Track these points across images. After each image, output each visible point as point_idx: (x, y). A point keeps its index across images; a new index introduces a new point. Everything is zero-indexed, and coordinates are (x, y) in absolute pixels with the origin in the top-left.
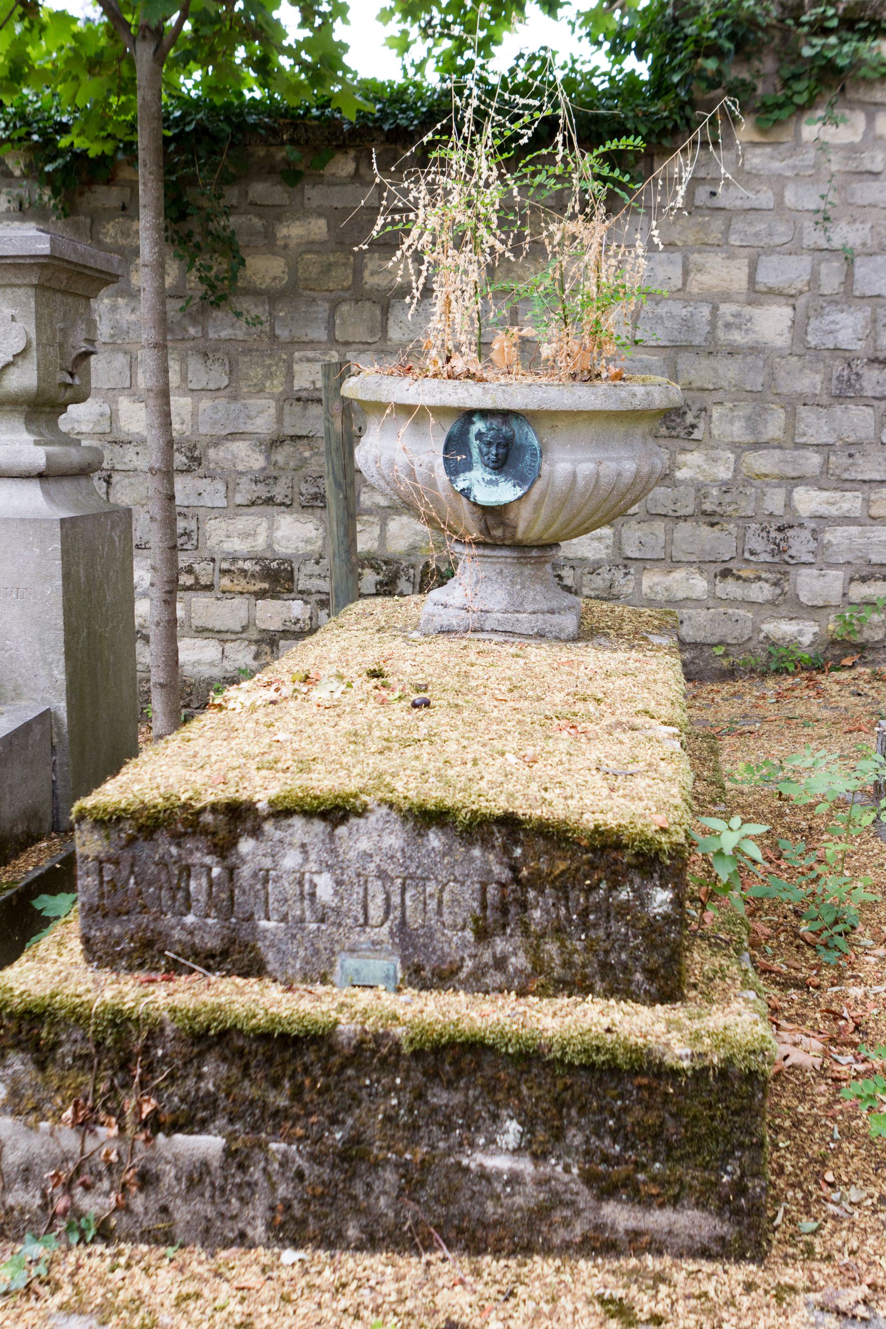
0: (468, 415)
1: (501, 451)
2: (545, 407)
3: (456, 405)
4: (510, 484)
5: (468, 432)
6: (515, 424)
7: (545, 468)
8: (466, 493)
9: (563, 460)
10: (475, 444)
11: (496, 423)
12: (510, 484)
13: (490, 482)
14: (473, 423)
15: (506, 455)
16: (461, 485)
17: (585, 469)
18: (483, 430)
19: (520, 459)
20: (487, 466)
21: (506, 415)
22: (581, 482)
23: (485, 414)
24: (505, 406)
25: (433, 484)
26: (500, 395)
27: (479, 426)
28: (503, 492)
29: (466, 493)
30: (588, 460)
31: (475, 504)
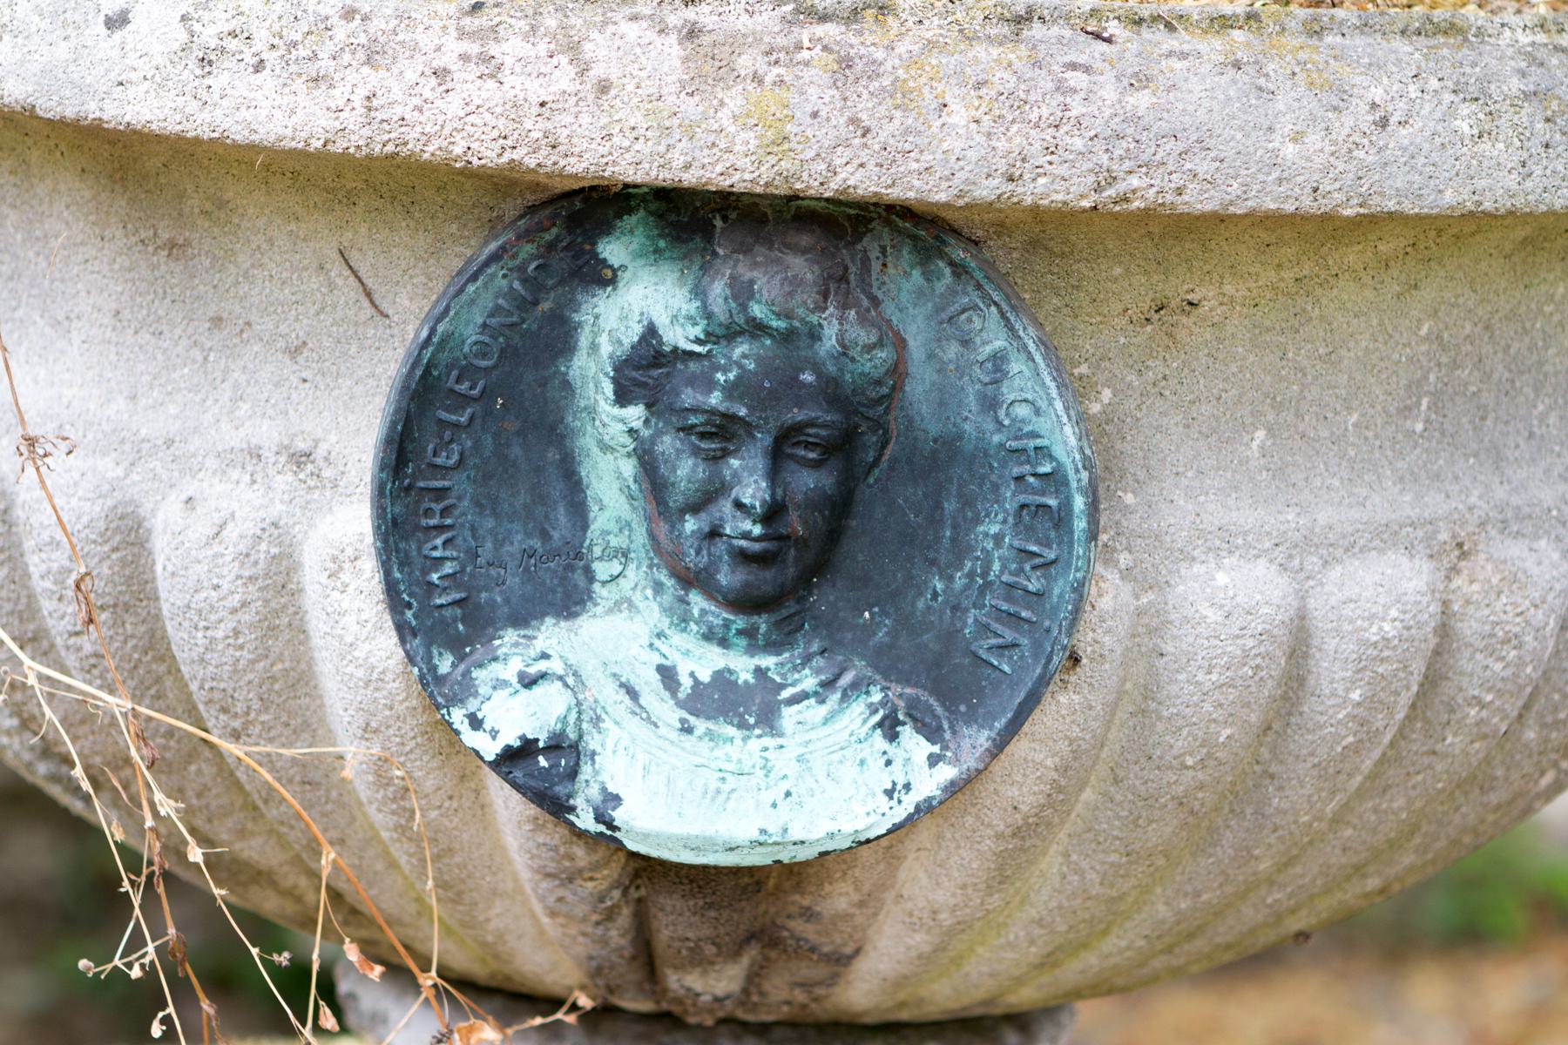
0: (571, 223)
1: (807, 481)
2: (1143, 189)
3: (489, 155)
4: (857, 716)
5: (558, 338)
6: (907, 291)
7: (1111, 595)
8: (542, 771)
9: (1227, 542)
10: (608, 431)
11: (775, 284)
12: (857, 716)
13: (719, 702)
14: (602, 277)
15: (838, 510)
16: (508, 715)
17: (1376, 598)
18: (680, 336)
19: (933, 540)
20: (689, 579)
21: (844, 232)
22: (1337, 689)
23: (691, 219)
24: (858, 176)
25: (288, 688)
26: (816, 89)
27: (645, 299)
28: (809, 775)
29: (542, 771)
30: (1387, 536)
31: (607, 841)
